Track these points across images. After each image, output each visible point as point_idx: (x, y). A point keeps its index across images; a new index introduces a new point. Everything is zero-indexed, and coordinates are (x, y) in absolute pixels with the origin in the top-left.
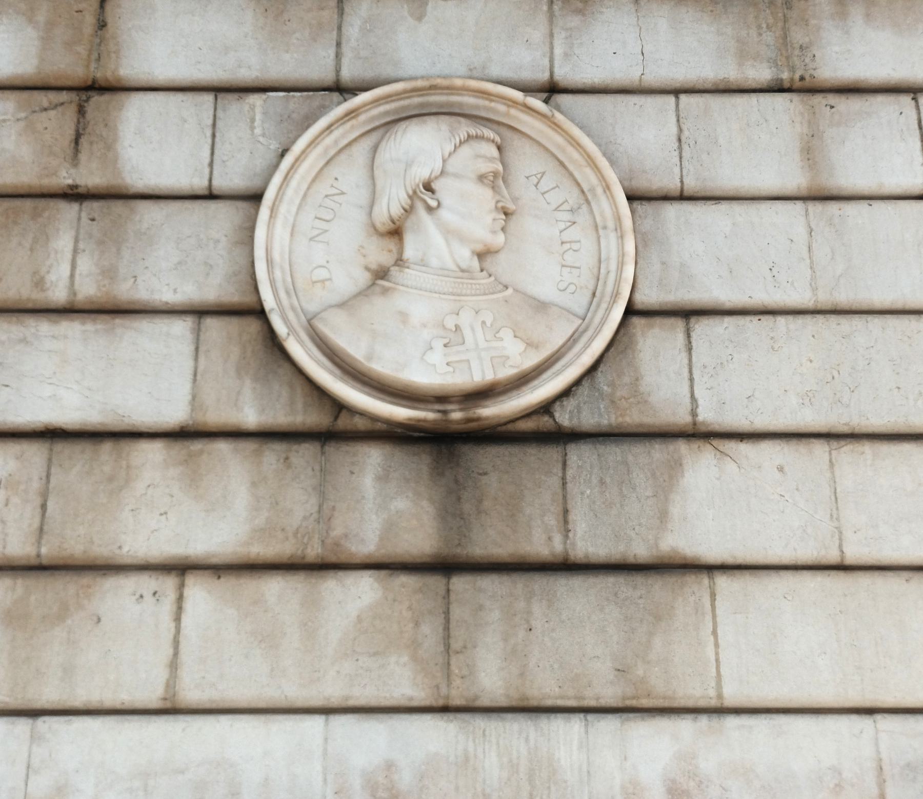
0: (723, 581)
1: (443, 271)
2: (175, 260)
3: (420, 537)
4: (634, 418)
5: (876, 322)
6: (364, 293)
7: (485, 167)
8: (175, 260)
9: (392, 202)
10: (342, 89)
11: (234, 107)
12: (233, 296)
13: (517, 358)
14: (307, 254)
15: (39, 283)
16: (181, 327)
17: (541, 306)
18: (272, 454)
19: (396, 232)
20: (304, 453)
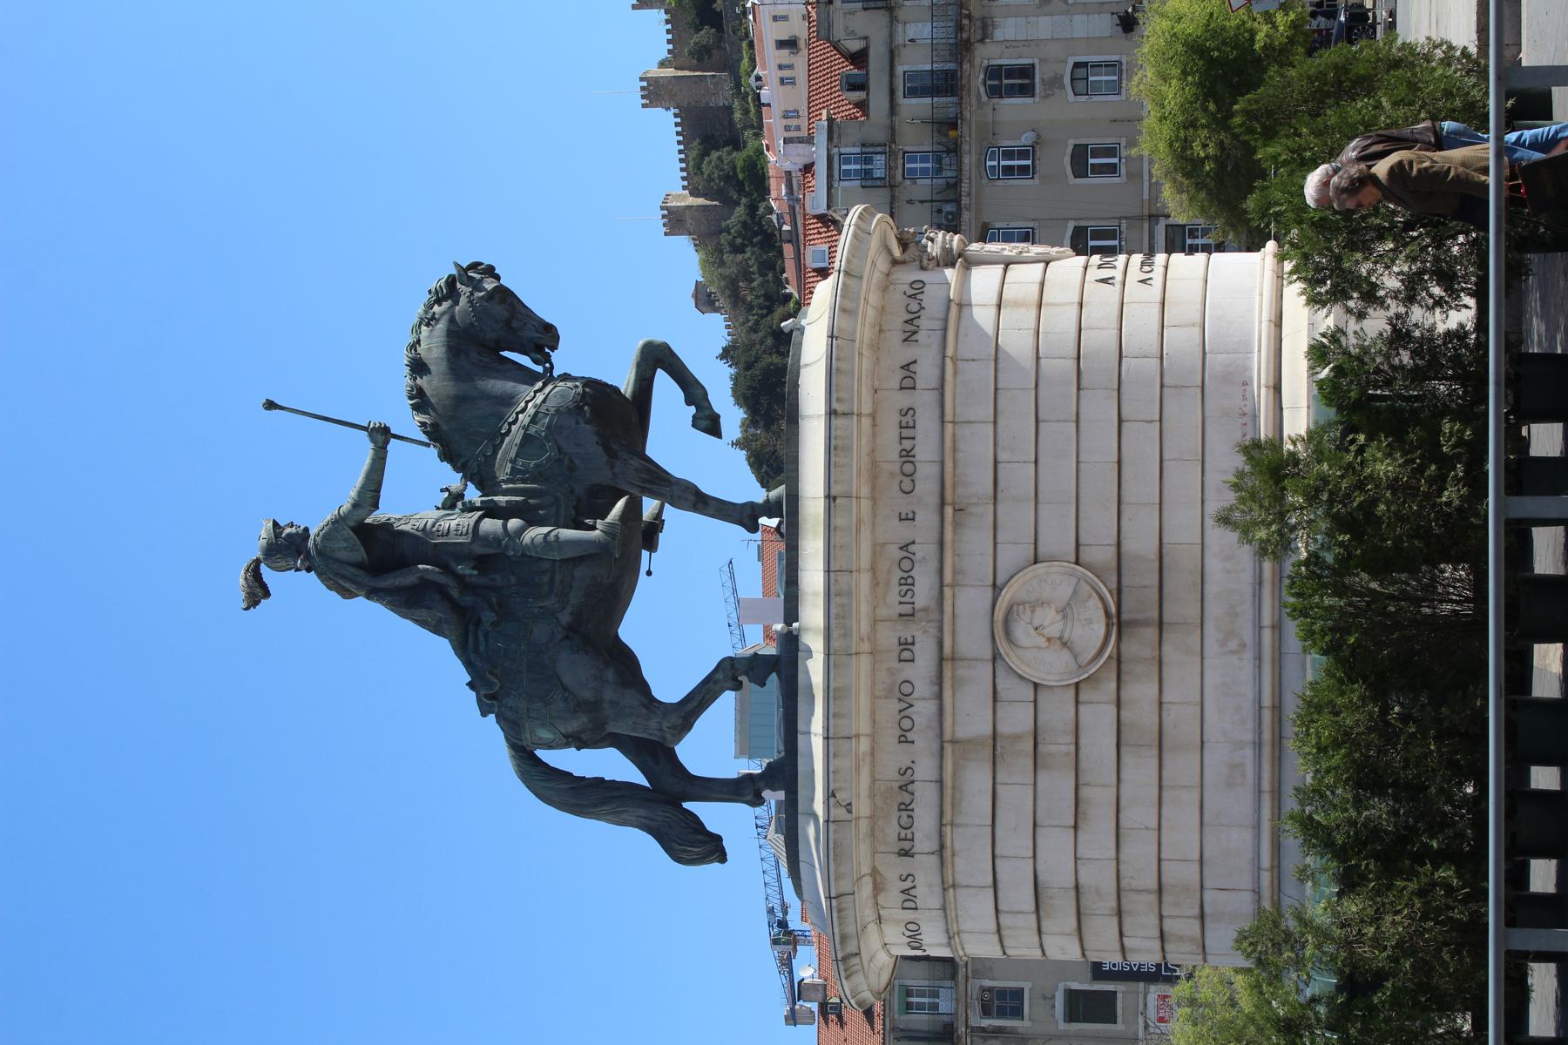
0: (1165, 541)
1: (1065, 625)
2: (1058, 711)
3: (1151, 633)
4: (1114, 564)
5: (1082, 485)
6: (1070, 649)
7: (1028, 611)
8: (1058, 711)
9: (1042, 642)
10: (996, 657)
11: (1001, 694)
12: (1072, 692)
13: (1095, 602)
14: (1052, 667)
15: (1068, 754)
16: (1082, 708)
17: (1075, 592)
18: (1124, 678)
19: (1049, 640)
20: (1123, 667)
